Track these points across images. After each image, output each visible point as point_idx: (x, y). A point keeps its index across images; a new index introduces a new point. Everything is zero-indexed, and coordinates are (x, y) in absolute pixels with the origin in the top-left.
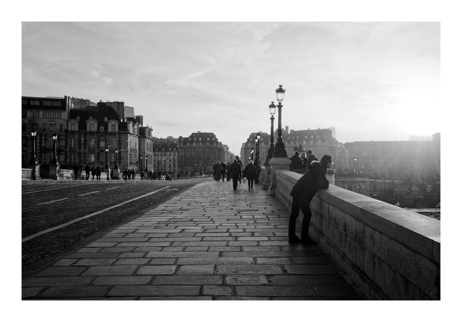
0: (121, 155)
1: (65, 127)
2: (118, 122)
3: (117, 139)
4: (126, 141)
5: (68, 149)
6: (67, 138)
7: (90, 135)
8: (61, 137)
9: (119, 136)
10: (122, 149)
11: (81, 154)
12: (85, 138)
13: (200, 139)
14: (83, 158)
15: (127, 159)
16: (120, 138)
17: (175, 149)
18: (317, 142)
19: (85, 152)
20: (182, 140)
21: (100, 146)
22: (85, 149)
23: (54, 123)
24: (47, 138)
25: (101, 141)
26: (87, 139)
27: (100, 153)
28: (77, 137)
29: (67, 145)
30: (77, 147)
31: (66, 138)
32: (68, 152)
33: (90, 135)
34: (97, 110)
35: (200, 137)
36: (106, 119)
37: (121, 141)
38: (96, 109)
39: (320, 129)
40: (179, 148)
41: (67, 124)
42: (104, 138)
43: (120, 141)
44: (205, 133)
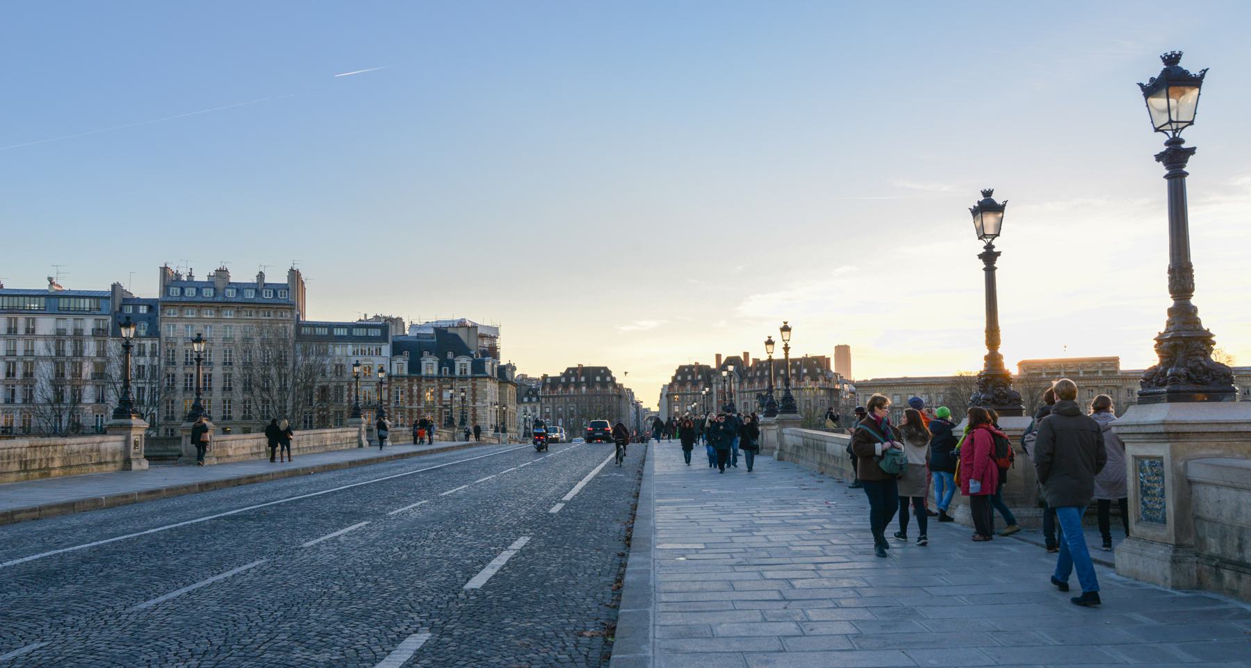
1: (387, 369)
2: (471, 359)
3: (470, 386)
4: (485, 390)
5: (392, 405)
6: (392, 387)
7: (427, 381)
10: (478, 404)
11: (413, 412)
12: (419, 386)
13: (583, 379)
15: (486, 419)
16: (474, 385)
17: (534, 399)
18: (803, 380)
19: (419, 409)
20: (549, 381)
21: (444, 399)
23: (371, 363)
25: (444, 390)
26: (422, 388)
27: (444, 410)
28: (406, 385)
31: (389, 387)
32: (393, 409)
33: (427, 381)
34: (435, 340)
35: (581, 376)
36: (450, 355)
37: (476, 389)
38: (433, 338)
39: (808, 357)
40: (542, 397)
41: (391, 364)
43: (474, 390)
44: (593, 368)
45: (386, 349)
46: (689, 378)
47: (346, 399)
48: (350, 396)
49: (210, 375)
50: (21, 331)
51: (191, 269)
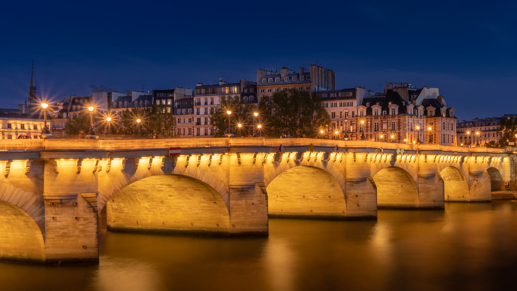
0: (401, 135)
1: (356, 114)
3: (397, 121)
4: (405, 122)
9: (398, 118)
10: (401, 130)
12: (371, 121)
16: (399, 120)
19: (371, 134)
21: (383, 128)
22: (371, 132)
24: (342, 123)
25: (383, 123)
29: (358, 129)
30: (365, 130)
31: (357, 122)
37: (400, 122)
41: (357, 110)
42: (386, 121)
43: (399, 123)
50: (209, 103)
51: (277, 68)
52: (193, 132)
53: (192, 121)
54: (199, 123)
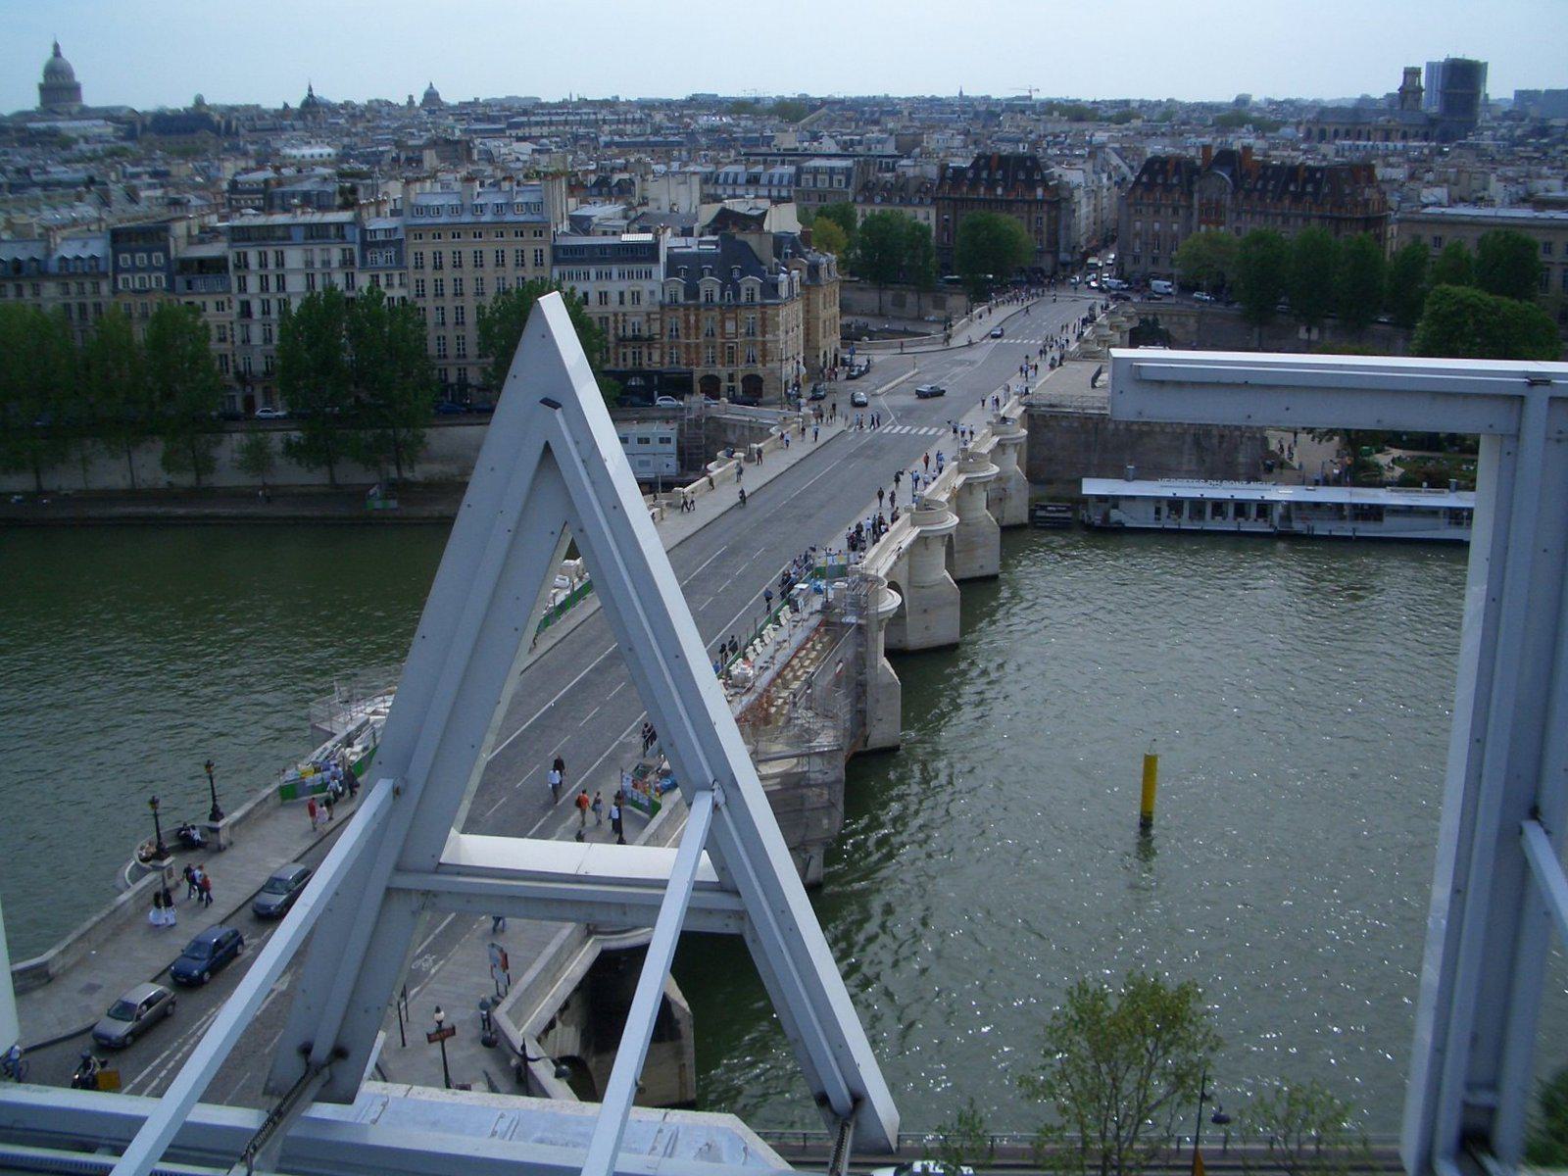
8: (652, 316)
10: (769, 337)
14: (693, 356)
19: (697, 345)
23: (637, 289)
43: (764, 319)
45: (659, 271)
46: (1160, 181)
47: (612, 332)
48: (616, 328)
49: (462, 308)
52: (233, 336)
53: (226, 308)
54: (246, 310)
